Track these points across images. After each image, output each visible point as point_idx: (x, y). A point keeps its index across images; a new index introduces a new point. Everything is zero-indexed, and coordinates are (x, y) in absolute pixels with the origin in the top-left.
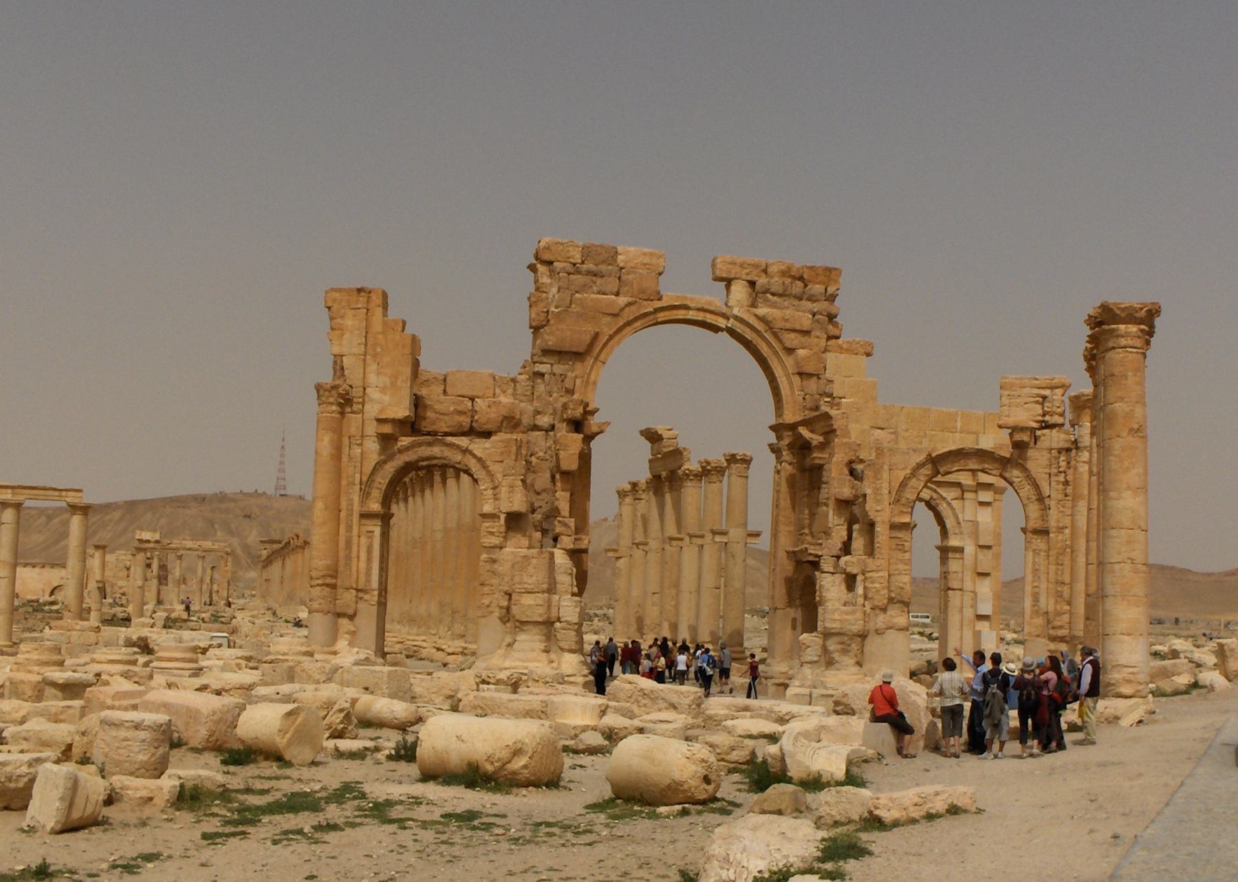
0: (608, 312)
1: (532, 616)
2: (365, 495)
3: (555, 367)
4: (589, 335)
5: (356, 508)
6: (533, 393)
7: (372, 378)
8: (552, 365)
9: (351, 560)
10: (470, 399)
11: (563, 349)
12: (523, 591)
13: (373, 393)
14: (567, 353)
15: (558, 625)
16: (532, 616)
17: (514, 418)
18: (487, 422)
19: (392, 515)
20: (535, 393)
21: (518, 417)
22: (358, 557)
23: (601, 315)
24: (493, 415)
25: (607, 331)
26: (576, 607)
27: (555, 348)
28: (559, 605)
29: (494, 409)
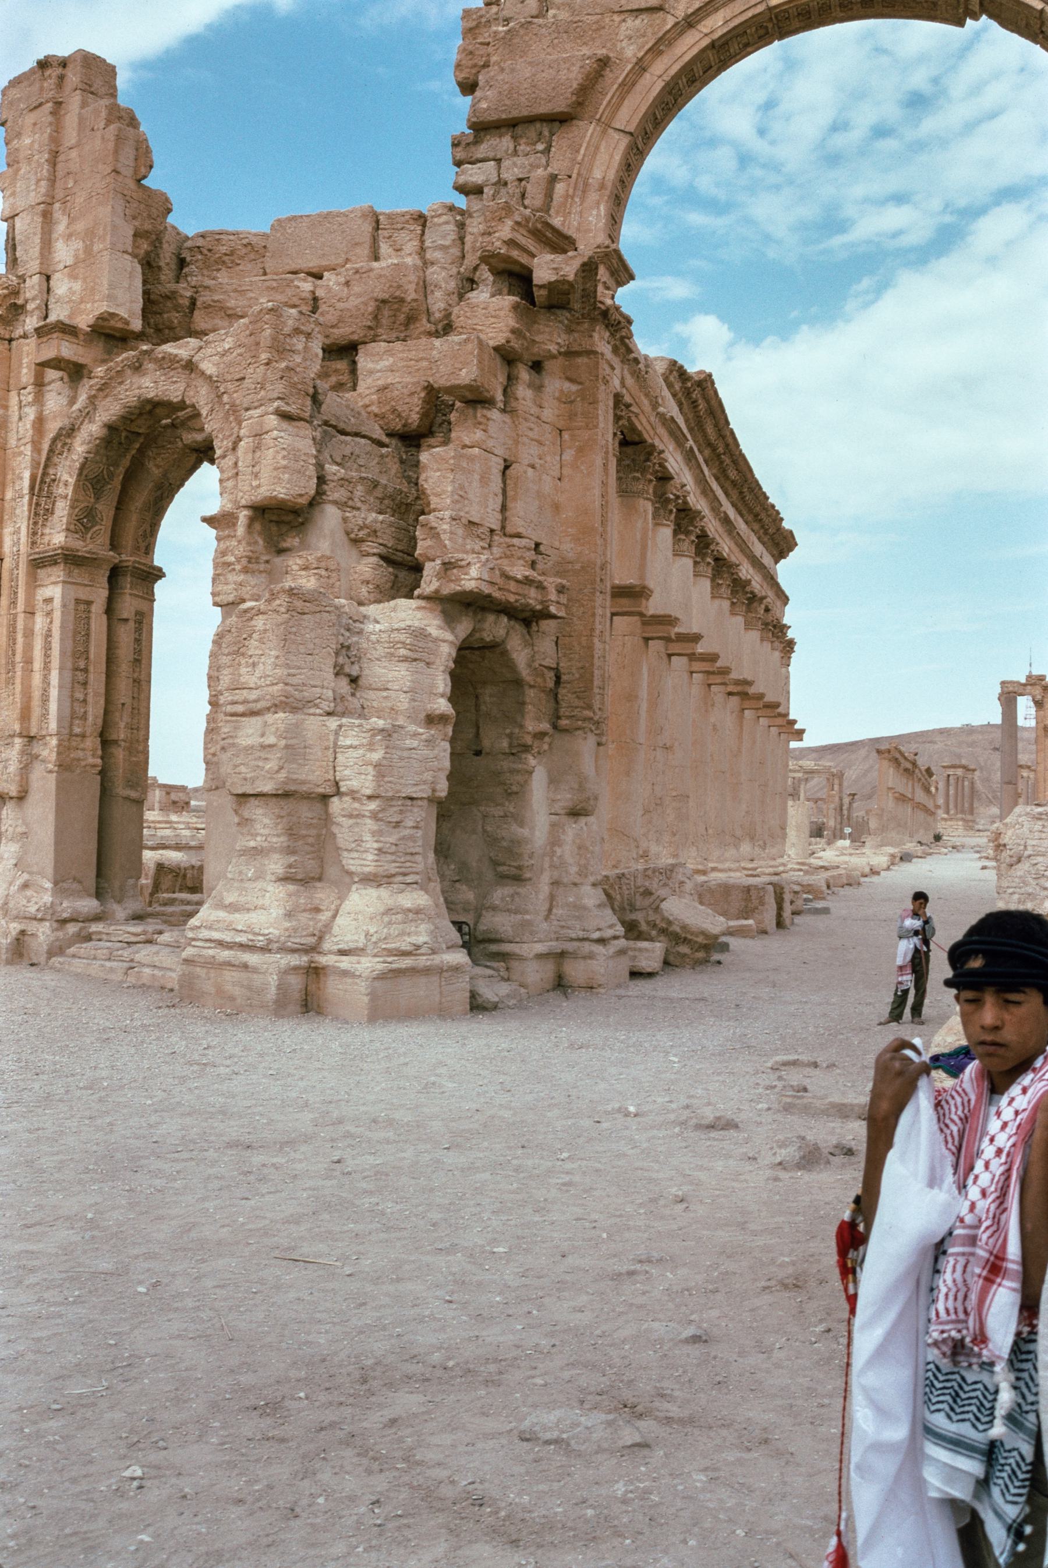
0: (629, 8)
1: (253, 780)
2: (40, 513)
3: (506, 163)
4: (575, 69)
5: (24, 548)
6: (462, 239)
7: (64, 253)
8: (499, 161)
9: (14, 666)
10: (311, 274)
11: (515, 114)
12: (240, 708)
13: (61, 286)
14: (530, 120)
15: (335, 804)
16: (253, 780)
17: (402, 300)
18: (341, 320)
19: (158, 574)
20: (468, 239)
21: (411, 295)
22: (28, 661)
23: (617, 18)
24: (353, 302)
25: (631, 52)
26: (371, 747)
27: (494, 117)
28: (335, 744)
29: (356, 289)
